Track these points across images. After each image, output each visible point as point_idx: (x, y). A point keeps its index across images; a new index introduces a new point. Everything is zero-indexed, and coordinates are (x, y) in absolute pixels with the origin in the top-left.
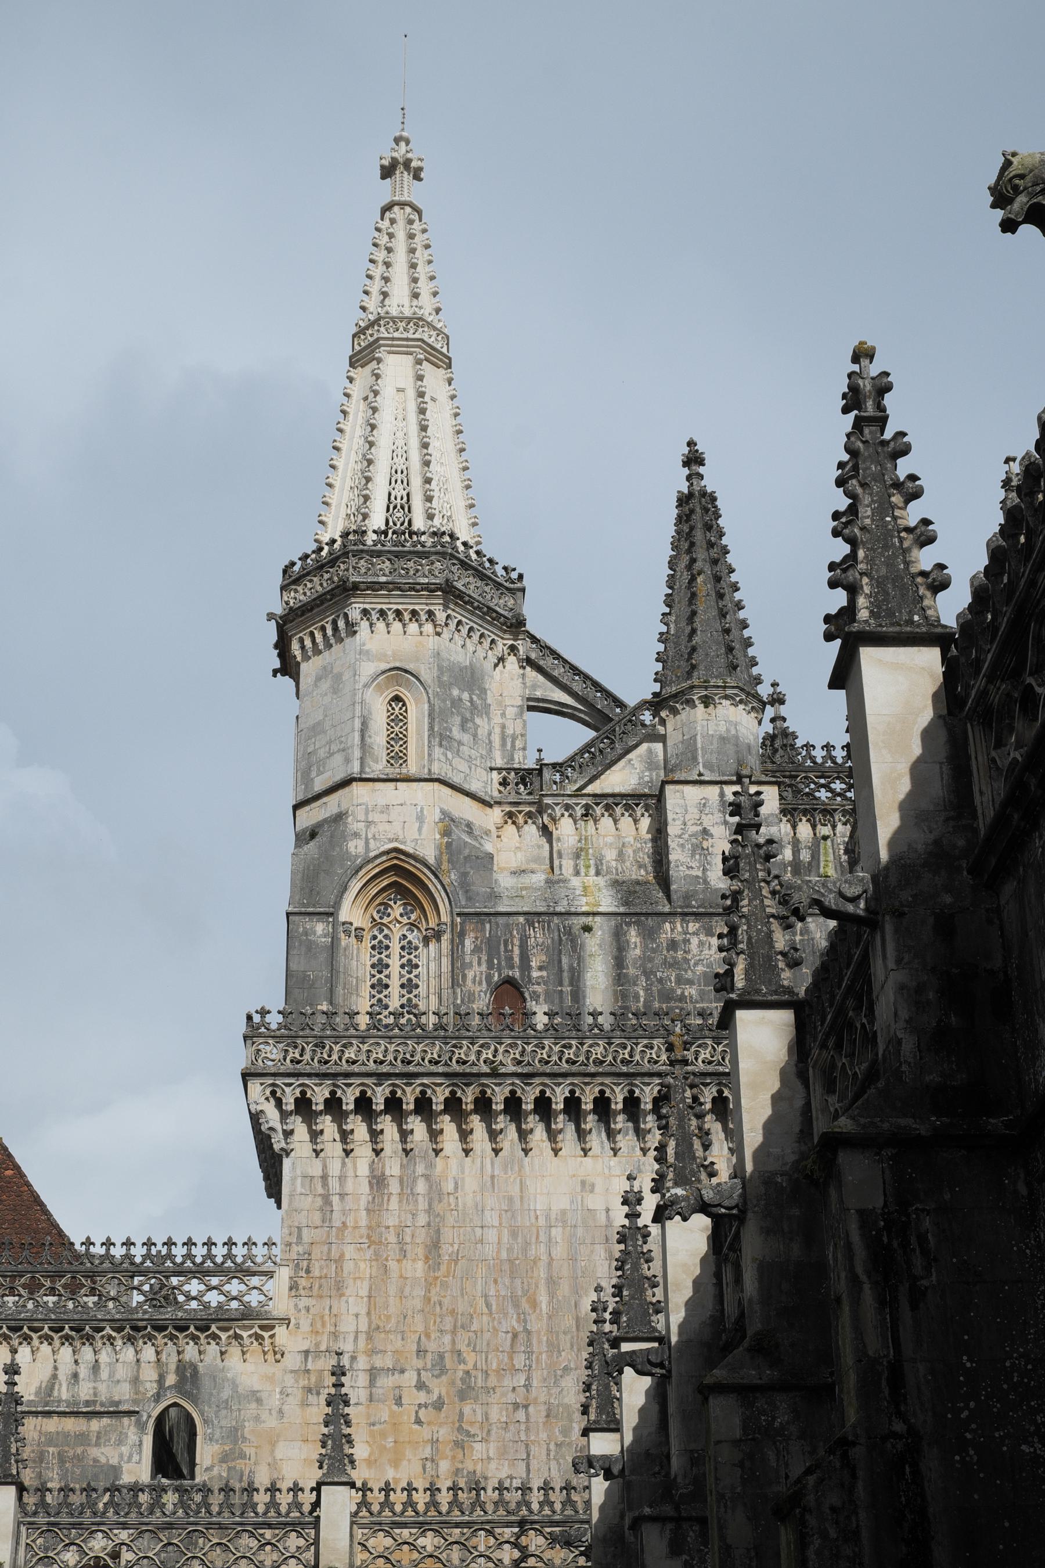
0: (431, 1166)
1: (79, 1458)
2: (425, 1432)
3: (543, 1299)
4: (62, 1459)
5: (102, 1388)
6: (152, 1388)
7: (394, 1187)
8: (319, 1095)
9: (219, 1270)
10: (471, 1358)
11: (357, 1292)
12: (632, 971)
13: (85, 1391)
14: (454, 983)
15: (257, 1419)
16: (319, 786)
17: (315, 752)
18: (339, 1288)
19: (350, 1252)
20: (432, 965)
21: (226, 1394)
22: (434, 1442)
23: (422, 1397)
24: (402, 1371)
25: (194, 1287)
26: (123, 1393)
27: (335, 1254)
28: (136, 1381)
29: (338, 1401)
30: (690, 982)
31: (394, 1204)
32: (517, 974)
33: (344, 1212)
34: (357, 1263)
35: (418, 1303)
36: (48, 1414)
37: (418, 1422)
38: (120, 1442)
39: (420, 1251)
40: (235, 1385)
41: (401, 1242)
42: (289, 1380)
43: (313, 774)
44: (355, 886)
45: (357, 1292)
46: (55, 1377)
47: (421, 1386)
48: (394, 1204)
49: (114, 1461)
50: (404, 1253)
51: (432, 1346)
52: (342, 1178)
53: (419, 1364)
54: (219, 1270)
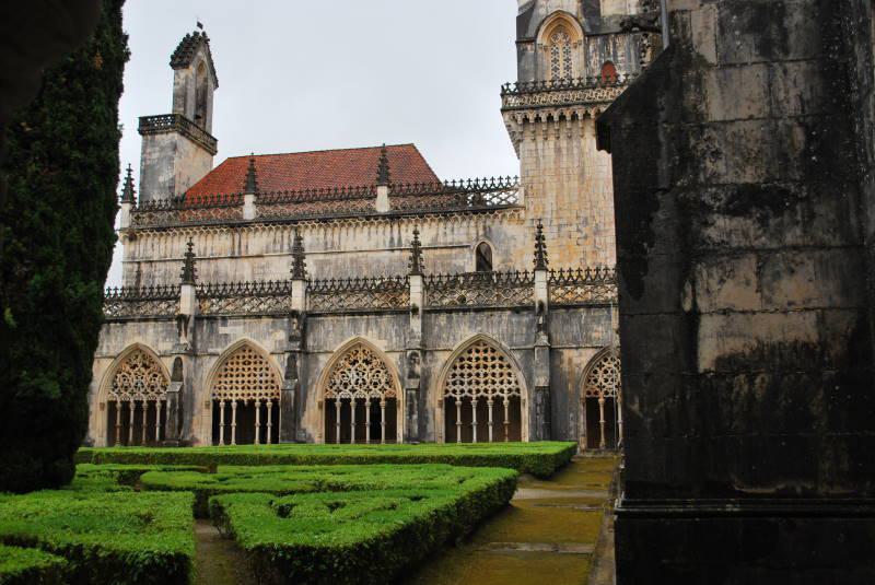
0: (580, 142)
1: (449, 264)
2: (581, 249)
4: (443, 265)
6: (474, 236)
7: (564, 152)
8: (531, 116)
9: (497, 189)
10: (598, 219)
13: (449, 239)
15: (515, 246)
18: (544, 194)
19: (548, 179)
23: (579, 235)
24: (571, 225)
25: (488, 197)
26: (463, 239)
27: (542, 180)
28: (468, 234)
29: (540, 238)
31: (565, 159)
33: (545, 163)
34: (551, 184)
35: (576, 198)
38: (464, 257)
40: (506, 235)
42: (527, 231)
44: (543, 28)
49: (462, 264)
50: (569, 178)
52: (543, 150)
54: (497, 189)
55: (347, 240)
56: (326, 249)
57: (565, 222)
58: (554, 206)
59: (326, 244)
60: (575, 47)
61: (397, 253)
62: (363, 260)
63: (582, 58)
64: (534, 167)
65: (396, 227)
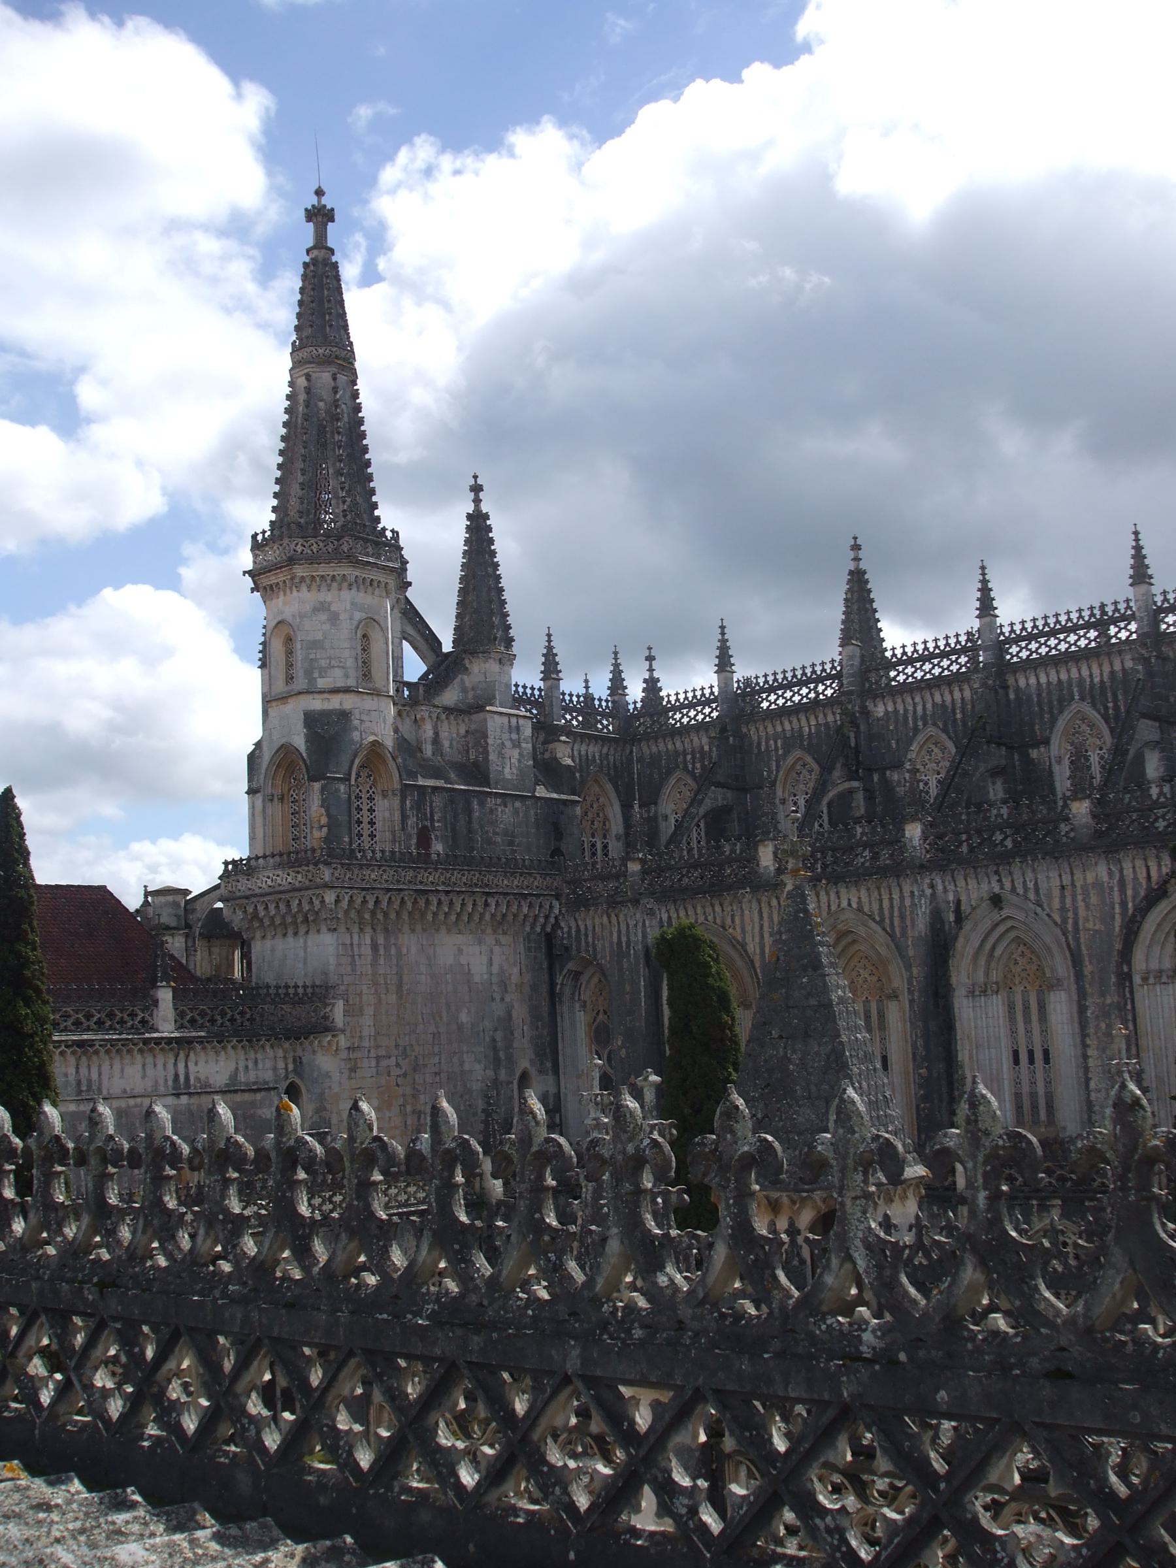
0: (396, 939)
2: (400, 1091)
3: (444, 1014)
5: (260, 1073)
6: (282, 1072)
7: (382, 951)
10: (417, 1048)
11: (369, 1011)
12: (476, 826)
14: (403, 829)
15: (330, 1087)
16: (321, 683)
17: (316, 660)
18: (361, 1011)
19: (364, 988)
20: (387, 814)
21: (315, 1074)
22: (404, 1095)
26: (268, 1076)
30: (498, 834)
31: (382, 962)
32: (428, 823)
36: (236, 1091)
37: (398, 1085)
39: (394, 988)
41: (386, 983)
43: (316, 675)
45: (369, 1011)
46: (237, 1069)
47: (398, 1065)
48: (382, 962)
51: (401, 1042)
52: (359, 945)
53: (396, 1052)
55: (111, 1077)
56: (80, 1092)
57: (384, 1053)
58: (373, 1029)
59: (79, 1083)
60: (385, 796)
61: (184, 1099)
62: (136, 1110)
63: (397, 816)
64: (349, 968)
65: (182, 1055)
